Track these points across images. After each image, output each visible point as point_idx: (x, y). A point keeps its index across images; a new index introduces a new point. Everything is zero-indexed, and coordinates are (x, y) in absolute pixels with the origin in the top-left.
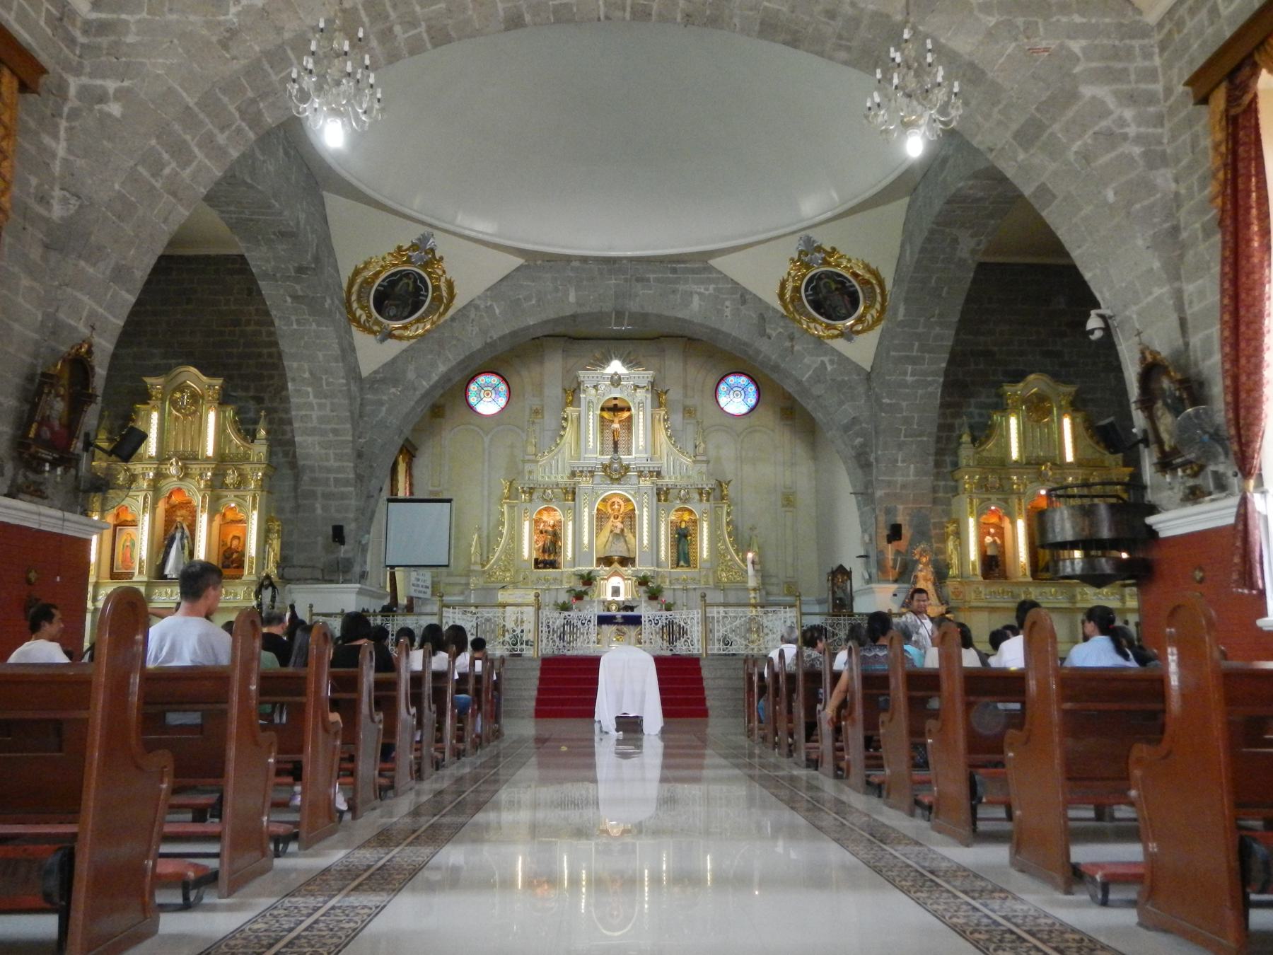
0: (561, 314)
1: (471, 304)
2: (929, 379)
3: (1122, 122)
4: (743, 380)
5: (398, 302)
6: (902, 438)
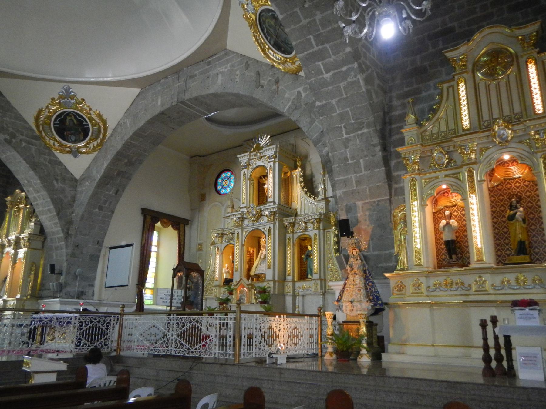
0: (154, 115)
1: (119, 124)
2: (344, 68)
5: (72, 132)
6: (345, 136)
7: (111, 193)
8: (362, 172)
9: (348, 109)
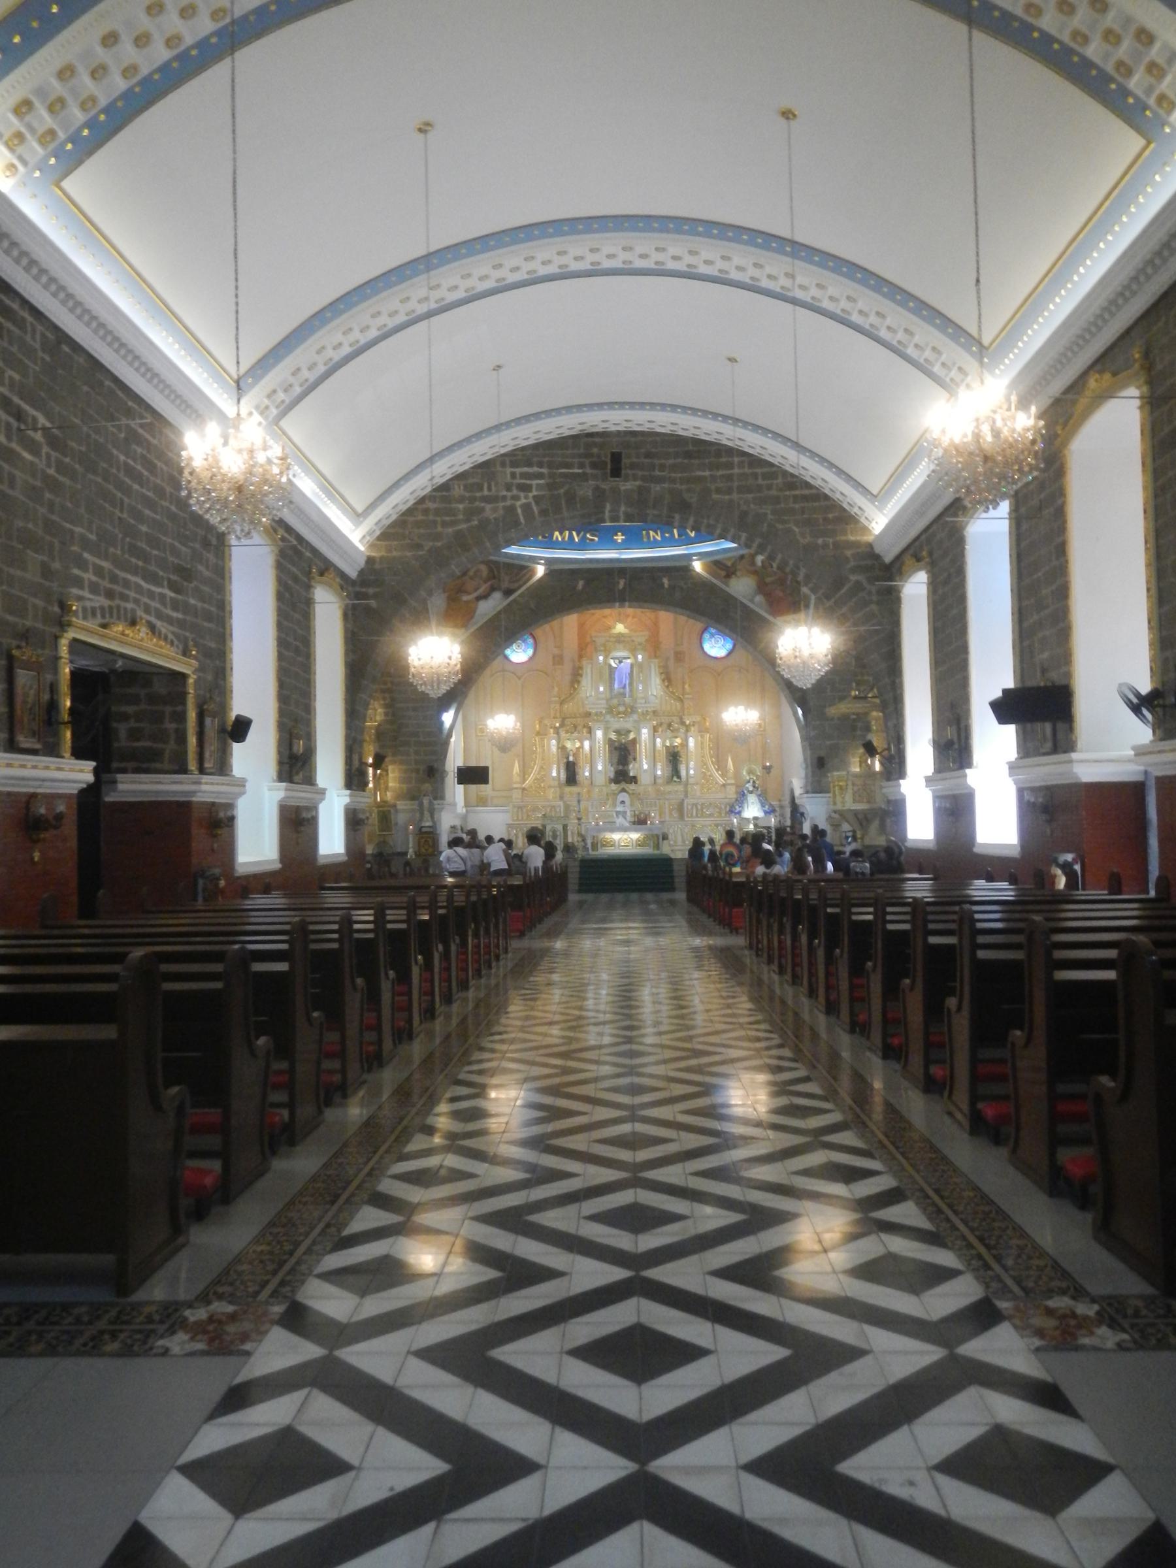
3: (870, 593)
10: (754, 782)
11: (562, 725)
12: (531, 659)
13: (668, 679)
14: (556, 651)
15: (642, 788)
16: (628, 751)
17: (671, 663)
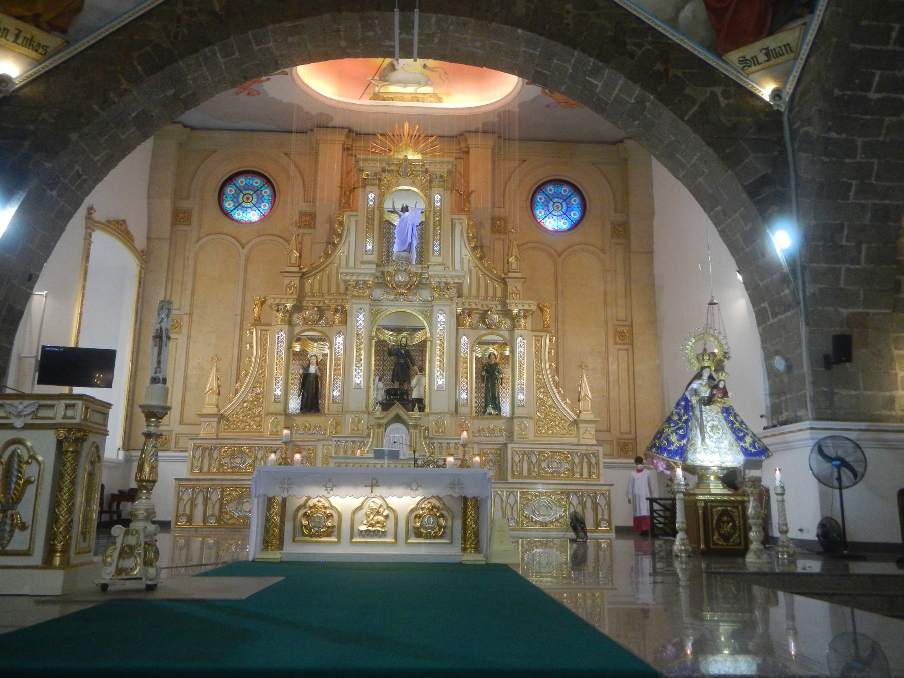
4: (565, 190)
7: (97, 158)
8: (860, 264)
9: (876, 161)
10: (711, 377)
11: (298, 308)
12: (264, 218)
13: (479, 247)
14: (305, 207)
15: (432, 418)
16: (410, 357)
17: (486, 232)
